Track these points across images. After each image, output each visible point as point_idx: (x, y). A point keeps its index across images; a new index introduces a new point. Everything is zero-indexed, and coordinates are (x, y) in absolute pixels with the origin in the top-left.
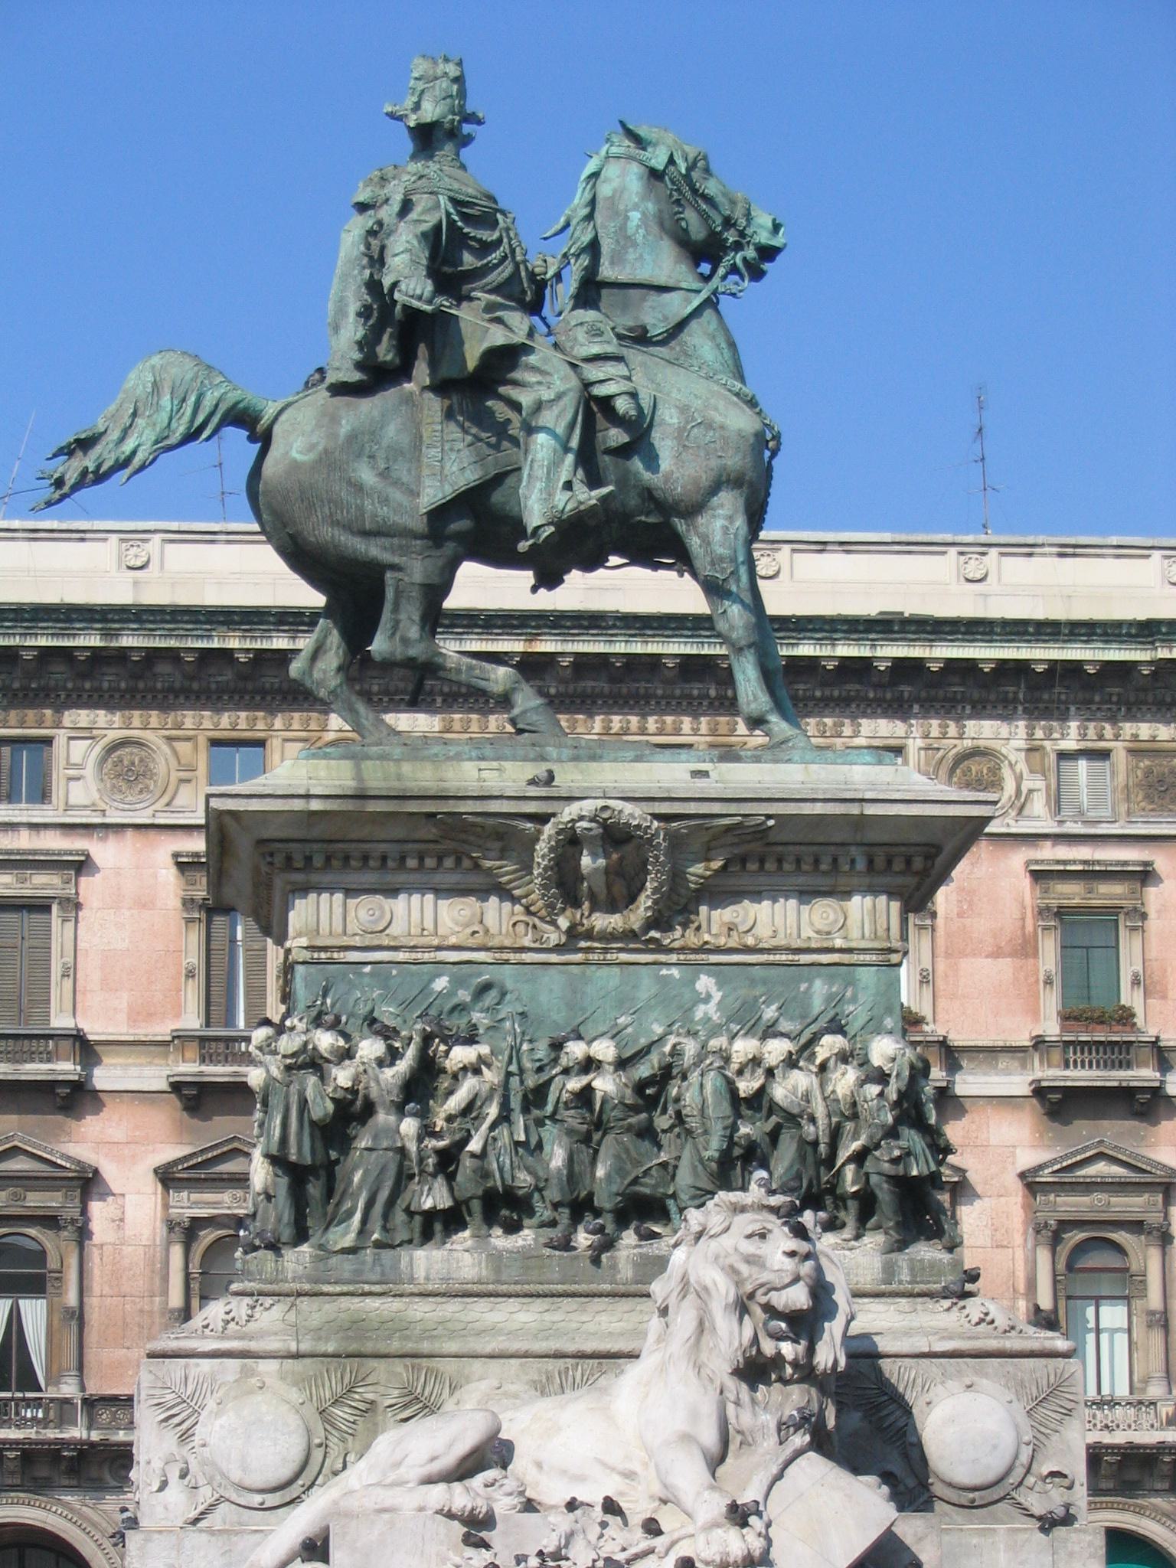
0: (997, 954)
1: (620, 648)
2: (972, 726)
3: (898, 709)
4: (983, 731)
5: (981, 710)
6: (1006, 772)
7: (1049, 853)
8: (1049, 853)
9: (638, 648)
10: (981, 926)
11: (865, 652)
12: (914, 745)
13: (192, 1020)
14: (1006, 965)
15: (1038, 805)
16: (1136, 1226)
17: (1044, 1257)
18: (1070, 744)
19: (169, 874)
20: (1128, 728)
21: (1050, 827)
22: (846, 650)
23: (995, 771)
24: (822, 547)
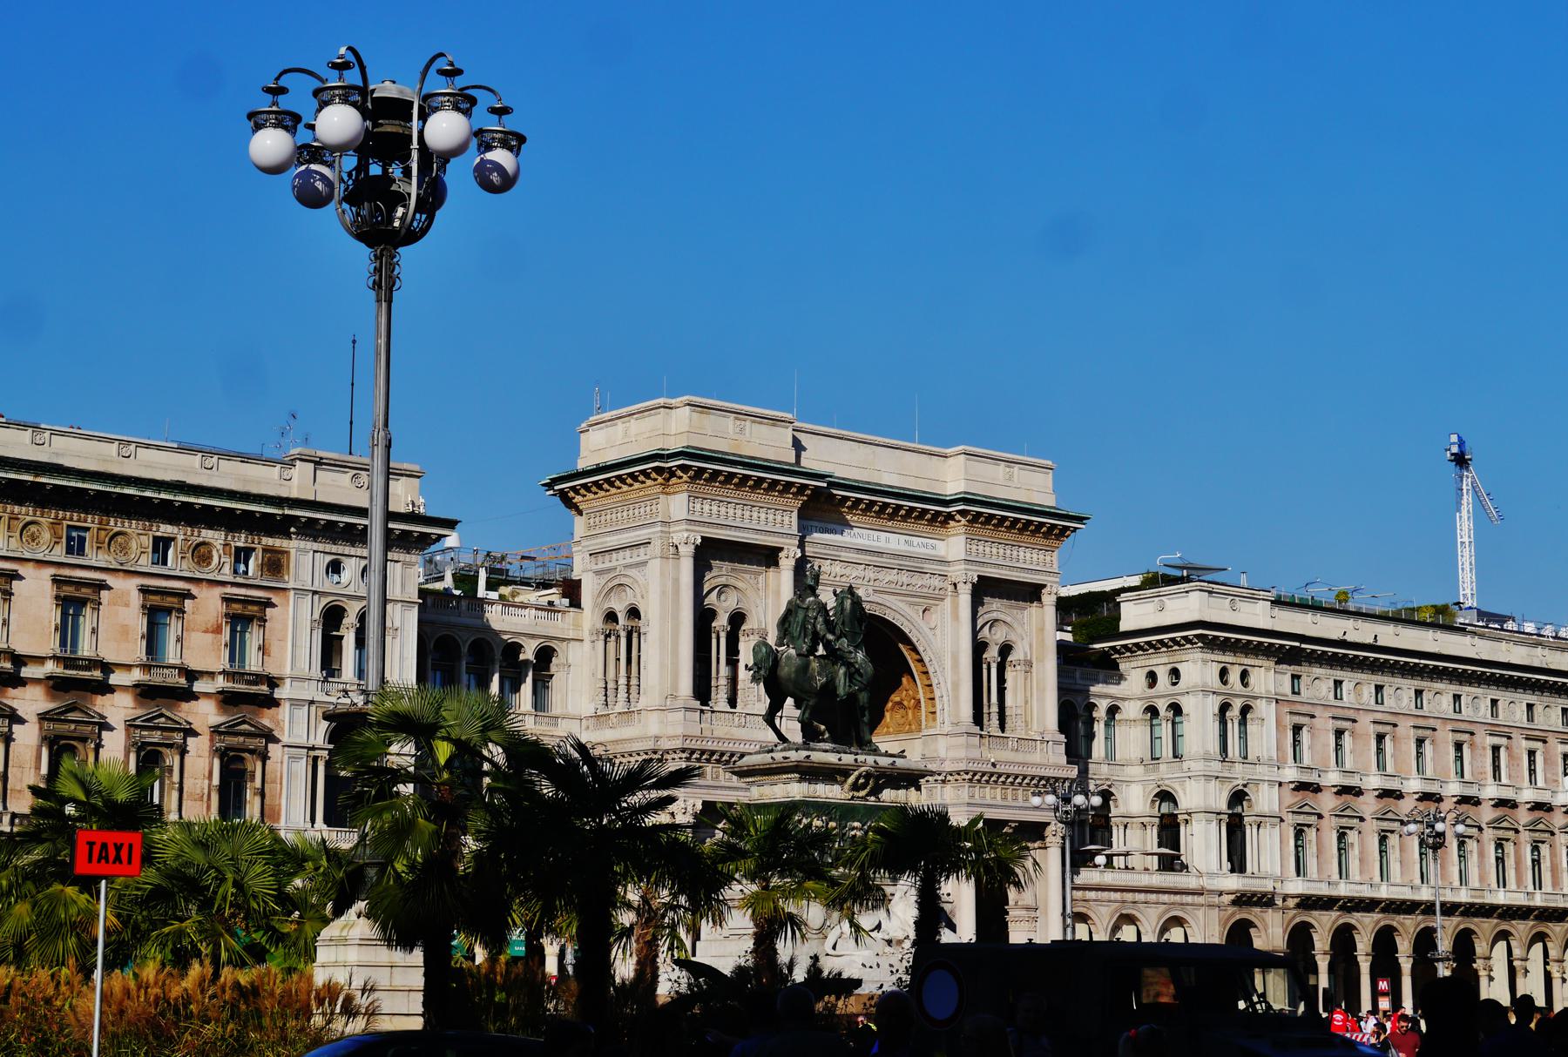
0: (206, 631)
1: (72, 484)
2: (204, 532)
3: (171, 521)
4: (208, 534)
6: (215, 553)
9: (80, 485)
11: (171, 497)
12: (180, 537)
14: (210, 636)
15: (227, 569)
16: (252, 752)
17: (217, 762)
18: (241, 544)
21: (230, 579)
24: (148, 446)
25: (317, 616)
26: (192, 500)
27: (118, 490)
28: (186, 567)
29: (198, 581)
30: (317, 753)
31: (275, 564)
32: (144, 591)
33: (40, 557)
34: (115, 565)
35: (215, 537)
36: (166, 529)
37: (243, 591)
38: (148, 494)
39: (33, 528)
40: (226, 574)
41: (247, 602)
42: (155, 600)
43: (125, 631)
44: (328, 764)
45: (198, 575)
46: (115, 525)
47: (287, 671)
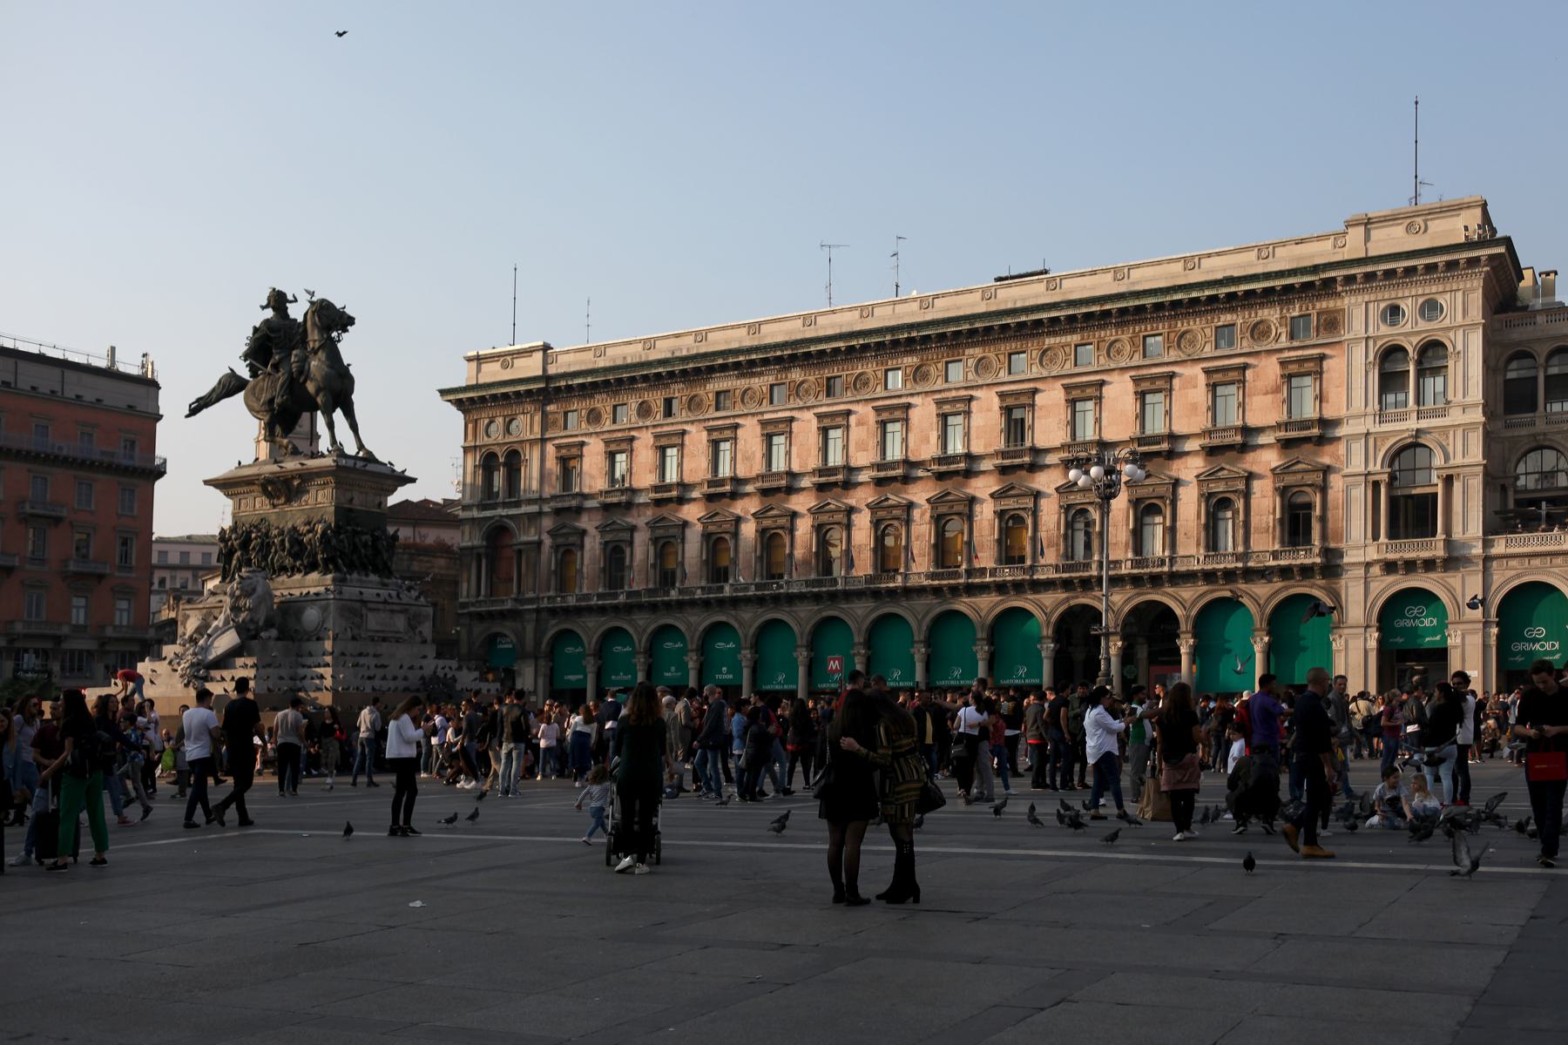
0: (1266, 393)
3: (1232, 310)
5: (1262, 305)
7: (1286, 354)
8: (1286, 354)
9: (1137, 303)
10: (1260, 384)
13: (1002, 446)
14: (1270, 397)
15: (1283, 338)
18: (1296, 314)
19: (996, 400)
20: (1318, 306)
22: (1207, 293)
23: (1269, 327)
25: (1371, 358)
26: (1233, 289)
27: (1168, 298)
28: (1246, 345)
29: (1257, 353)
30: (1376, 478)
31: (1332, 323)
32: (1207, 372)
33: (1123, 365)
34: (1184, 357)
35: (1271, 314)
36: (1227, 318)
37: (1300, 353)
38: (1194, 295)
39: (1118, 345)
40: (1284, 341)
41: (1301, 361)
42: (1218, 377)
43: (1194, 407)
44: (1390, 485)
45: (1257, 349)
46: (1181, 326)
47: (1343, 413)
